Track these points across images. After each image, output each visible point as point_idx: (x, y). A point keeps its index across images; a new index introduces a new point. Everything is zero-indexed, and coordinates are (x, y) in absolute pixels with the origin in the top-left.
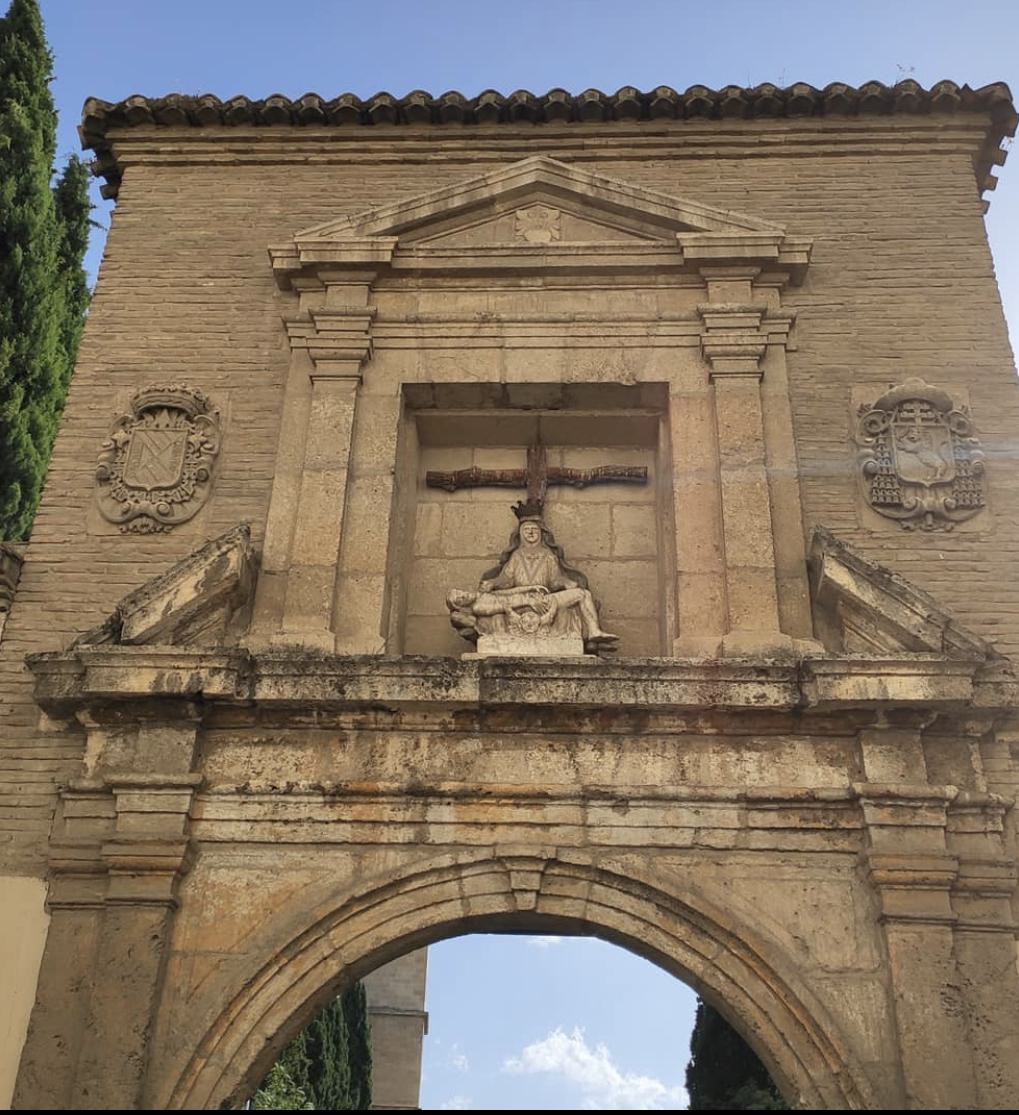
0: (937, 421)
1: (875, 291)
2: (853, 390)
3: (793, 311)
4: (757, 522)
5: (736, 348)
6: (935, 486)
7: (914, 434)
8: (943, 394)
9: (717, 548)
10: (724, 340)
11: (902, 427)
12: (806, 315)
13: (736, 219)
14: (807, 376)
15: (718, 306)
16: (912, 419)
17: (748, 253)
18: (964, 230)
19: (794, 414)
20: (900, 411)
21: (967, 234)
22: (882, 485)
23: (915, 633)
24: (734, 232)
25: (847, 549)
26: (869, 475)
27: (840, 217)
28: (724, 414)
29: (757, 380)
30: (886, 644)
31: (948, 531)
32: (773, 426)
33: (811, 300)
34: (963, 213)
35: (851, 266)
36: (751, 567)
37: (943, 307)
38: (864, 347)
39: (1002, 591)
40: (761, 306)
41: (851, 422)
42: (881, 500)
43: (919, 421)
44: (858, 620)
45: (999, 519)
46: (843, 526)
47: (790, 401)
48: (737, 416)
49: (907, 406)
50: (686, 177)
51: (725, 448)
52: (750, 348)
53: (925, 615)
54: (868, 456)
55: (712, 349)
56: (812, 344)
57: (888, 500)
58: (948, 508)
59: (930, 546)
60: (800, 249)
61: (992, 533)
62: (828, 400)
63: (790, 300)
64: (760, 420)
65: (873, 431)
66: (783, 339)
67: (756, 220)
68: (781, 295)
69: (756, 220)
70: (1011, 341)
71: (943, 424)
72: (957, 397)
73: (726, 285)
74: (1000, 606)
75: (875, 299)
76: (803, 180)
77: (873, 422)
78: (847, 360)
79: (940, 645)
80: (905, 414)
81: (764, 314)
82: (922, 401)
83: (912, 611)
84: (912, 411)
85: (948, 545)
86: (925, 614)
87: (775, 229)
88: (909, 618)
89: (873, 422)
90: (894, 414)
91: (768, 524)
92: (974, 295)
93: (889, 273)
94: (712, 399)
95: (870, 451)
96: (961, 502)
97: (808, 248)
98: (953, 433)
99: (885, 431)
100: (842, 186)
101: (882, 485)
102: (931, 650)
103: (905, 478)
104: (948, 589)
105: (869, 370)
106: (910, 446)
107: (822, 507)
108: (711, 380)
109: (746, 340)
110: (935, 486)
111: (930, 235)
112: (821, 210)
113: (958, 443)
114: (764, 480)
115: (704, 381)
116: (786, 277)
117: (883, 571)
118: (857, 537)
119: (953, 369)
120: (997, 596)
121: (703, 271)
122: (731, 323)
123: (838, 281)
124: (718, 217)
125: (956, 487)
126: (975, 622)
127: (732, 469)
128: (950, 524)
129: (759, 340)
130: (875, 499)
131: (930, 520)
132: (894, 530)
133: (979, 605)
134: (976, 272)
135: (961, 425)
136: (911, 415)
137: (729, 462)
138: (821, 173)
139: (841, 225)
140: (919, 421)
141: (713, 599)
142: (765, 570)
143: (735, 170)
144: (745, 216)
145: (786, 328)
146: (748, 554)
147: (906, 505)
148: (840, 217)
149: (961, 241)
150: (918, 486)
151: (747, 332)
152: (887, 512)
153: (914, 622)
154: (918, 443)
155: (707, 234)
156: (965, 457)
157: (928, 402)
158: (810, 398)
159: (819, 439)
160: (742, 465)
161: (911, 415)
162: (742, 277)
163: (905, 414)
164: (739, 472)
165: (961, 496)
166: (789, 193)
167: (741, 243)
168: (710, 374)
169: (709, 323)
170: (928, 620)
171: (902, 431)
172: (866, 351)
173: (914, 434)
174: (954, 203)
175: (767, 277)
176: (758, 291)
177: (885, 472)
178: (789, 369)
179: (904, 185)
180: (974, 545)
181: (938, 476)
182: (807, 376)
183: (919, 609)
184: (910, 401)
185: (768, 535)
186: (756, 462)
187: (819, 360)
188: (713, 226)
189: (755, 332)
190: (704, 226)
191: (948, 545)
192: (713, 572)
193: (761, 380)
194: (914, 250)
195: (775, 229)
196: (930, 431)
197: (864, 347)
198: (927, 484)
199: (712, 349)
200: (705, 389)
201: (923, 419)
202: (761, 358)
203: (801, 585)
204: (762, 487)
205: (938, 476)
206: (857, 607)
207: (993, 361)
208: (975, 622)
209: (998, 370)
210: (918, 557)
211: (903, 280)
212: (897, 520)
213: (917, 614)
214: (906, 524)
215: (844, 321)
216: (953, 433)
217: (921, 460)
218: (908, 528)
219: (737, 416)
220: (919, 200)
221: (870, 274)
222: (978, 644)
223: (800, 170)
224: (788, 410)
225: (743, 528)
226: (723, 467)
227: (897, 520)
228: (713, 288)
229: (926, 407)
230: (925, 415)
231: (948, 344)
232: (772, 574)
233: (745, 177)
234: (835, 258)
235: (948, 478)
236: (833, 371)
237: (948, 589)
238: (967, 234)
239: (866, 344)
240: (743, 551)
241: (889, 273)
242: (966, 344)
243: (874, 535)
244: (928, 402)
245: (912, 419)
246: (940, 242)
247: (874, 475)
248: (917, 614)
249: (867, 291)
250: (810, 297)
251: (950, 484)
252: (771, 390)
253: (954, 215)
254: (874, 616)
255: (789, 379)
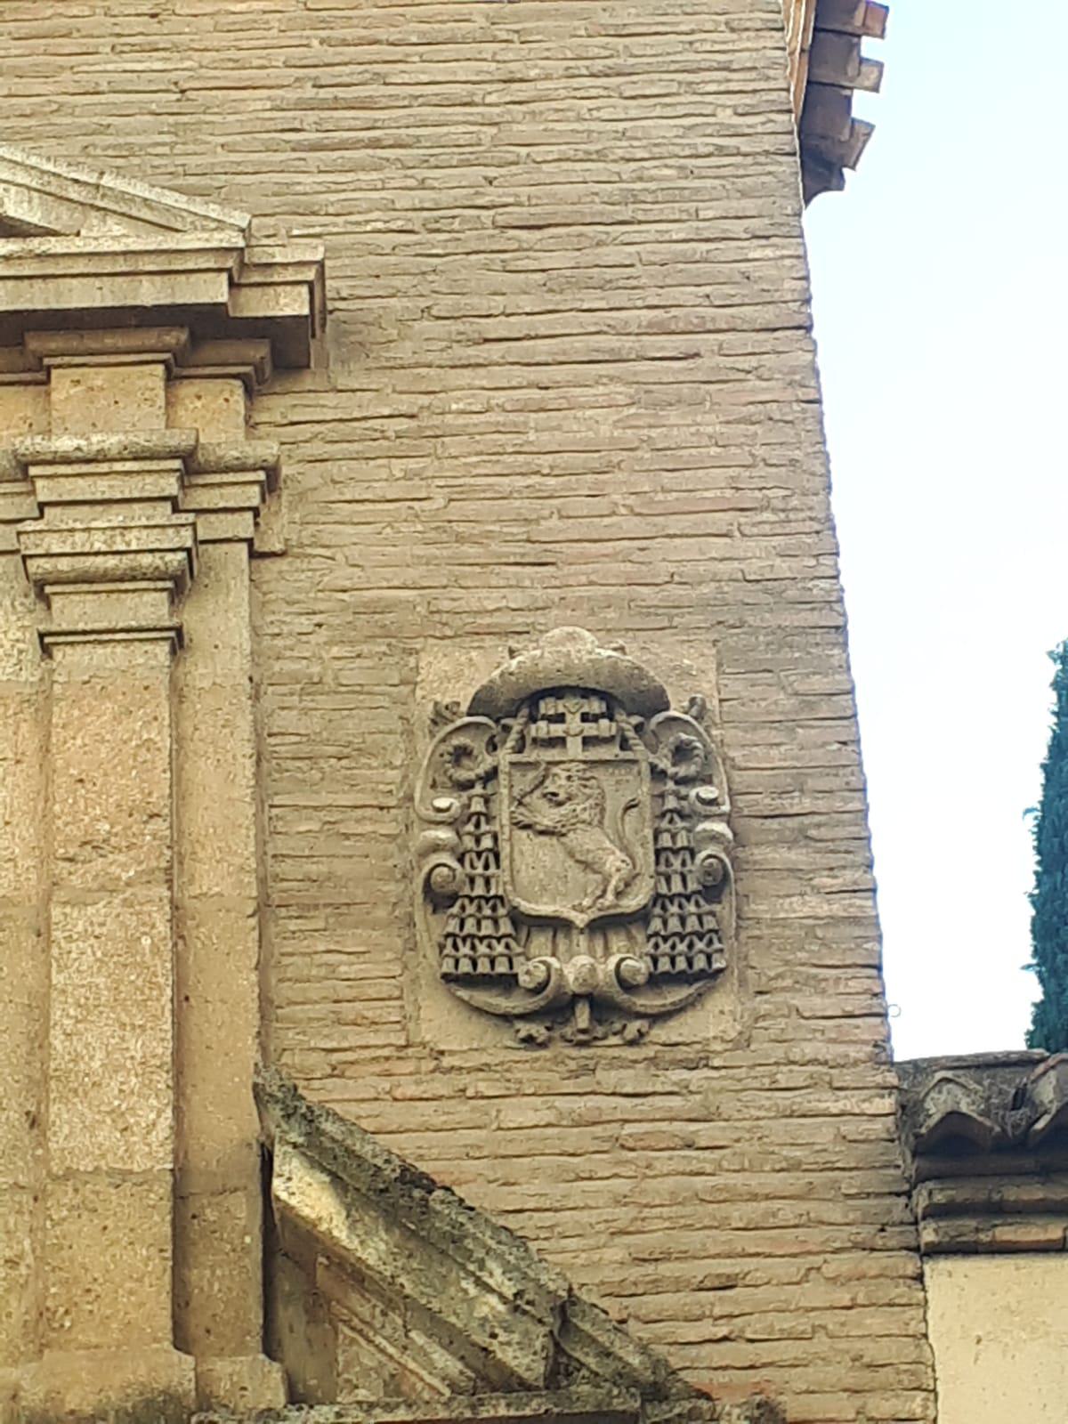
0: (624, 745)
1: (501, 375)
2: (425, 660)
3: (267, 449)
4: (135, 1047)
5: (111, 562)
6: (603, 926)
7: (558, 784)
8: (637, 672)
9: (34, 1121)
10: (80, 542)
11: (533, 765)
12: (317, 449)
13: (123, 196)
14: (305, 623)
15: (65, 444)
16: (559, 742)
17: (149, 294)
18: (744, 194)
19: (261, 734)
20: (533, 719)
21: (749, 206)
22: (470, 927)
23: (481, 1339)
24: (111, 235)
25: (328, 1126)
26: (439, 898)
27: (424, 162)
28: (72, 749)
29: (166, 647)
30: (431, 1366)
31: (632, 1043)
32: (202, 771)
33: (332, 404)
34: (744, 145)
35: (444, 305)
36: (111, 1173)
37: (673, 415)
38: (460, 539)
39: (754, 1197)
40: (179, 439)
41: (411, 752)
42: (465, 966)
43: (574, 748)
44: (364, 1307)
45: (763, 1005)
46: (373, 1039)
47: (256, 697)
48: (104, 751)
49: (547, 707)
50: (17, 48)
51: (68, 840)
52: (146, 560)
53: (509, 1293)
54: (436, 848)
55: (46, 564)
56: (328, 533)
57: (484, 967)
58: (626, 985)
59: (585, 1083)
60: (290, 275)
61: (743, 1042)
62: (360, 690)
63: (276, 407)
64: (162, 761)
65: (463, 775)
66: (242, 525)
67: (170, 198)
68: (249, 393)
69: (170, 198)
70: (835, 509)
71: (639, 750)
72: (686, 673)
73: (99, 377)
74: (748, 1241)
75: (500, 397)
76: (330, 54)
77: (461, 754)
78: (411, 575)
79: (540, 1368)
80: (542, 729)
81: (191, 465)
82: (586, 693)
83: (479, 1282)
84: (560, 718)
85: (630, 1080)
86: (509, 1290)
87: (221, 225)
88: (470, 1302)
89: (461, 754)
90: (516, 724)
91: (164, 1050)
92: (754, 383)
93: (542, 324)
94: (42, 701)
95: (444, 834)
96: (664, 965)
97: (310, 274)
98: (658, 774)
99: (493, 774)
100: (438, 71)
101: (470, 927)
102: (524, 1386)
103: (527, 907)
104: (620, 1201)
105: (471, 600)
106: (548, 816)
107: (314, 991)
108: (46, 651)
109: (134, 540)
110: (603, 926)
111: (656, 211)
112: (375, 144)
113: (671, 803)
114: (163, 928)
115: (34, 650)
116: (260, 351)
117: (412, 1179)
118: (409, 1066)
119: (680, 591)
120: (739, 1213)
121: (34, 344)
122: (102, 489)
123: (404, 352)
124: (73, 193)
125: (656, 924)
126: (678, 1285)
127: (79, 903)
128: (633, 1027)
129: (170, 539)
130: (448, 966)
131: (583, 1017)
132: (497, 1045)
133: (693, 1240)
134: (767, 315)
135: (682, 752)
136: (557, 730)
137: (75, 880)
138: (381, 34)
139: (422, 185)
140: (574, 748)
141: (12, 1263)
142: (146, 1179)
143: (154, 25)
144: (140, 189)
145: (253, 496)
146: (107, 1135)
147: (524, 979)
148: (424, 162)
149: (737, 227)
150: (557, 925)
151: (140, 514)
152: (482, 998)
153: (482, 1311)
154: (567, 807)
155: (36, 244)
156: (682, 841)
157: (602, 695)
158: (313, 685)
159: (324, 799)
160: (109, 888)
161: (557, 730)
162: (140, 356)
163: (542, 729)
164: (97, 911)
165: (665, 948)
166: (291, 95)
167: (129, 265)
168: (42, 636)
169: (44, 491)
170: (516, 1305)
171: (531, 775)
172: (468, 549)
173: (558, 783)
174: (725, 116)
175: (209, 352)
176: (187, 390)
177: (479, 890)
178: (259, 605)
179: (598, 65)
180: (696, 1077)
181: (610, 897)
182: (305, 623)
183: (497, 1278)
184: (558, 692)
185: (163, 1079)
186: (147, 878)
187: (343, 576)
188: (60, 217)
189: (163, 513)
190: (34, 217)
191: (630, 1080)
192: (17, 1186)
193: (178, 641)
194: (612, 254)
195: (221, 225)
196: (598, 773)
197: (460, 539)
198: (580, 919)
199: (46, 564)
200: (30, 675)
201: (587, 742)
202: (179, 586)
203: (243, 1212)
204: (155, 950)
205: (610, 897)
206: (357, 1276)
207: (783, 567)
208: (678, 1285)
209: (792, 593)
210: (550, 1116)
211: (578, 343)
212: (507, 1018)
213: (491, 1290)
214: (525, 1029)
215: (412, 464)
216: (658, 774)
217: (571, 854)
218: (529, 1040)
219: (104, 751)
220: (634, 108)
221: (494, 328)
222: (635, 1361)
223: (326, 24)
224: (244, 724)
225: (96, 1064)
226: (60, 895)
227: (507, 1018)
228: (62, 384)
229: (596, 706)
230: (590, 729)
231: (676, 524)
232: (163, 1189)
233: (175, 48)
234: (397, 282)
235: (632, 903)
236: (373, 609)
237: (620, 1201)
238: (749, 206)
239: (461, 528)
240: (90, 1129)
241: (542, 324)
242: (722, 520)
243: (447, 1061)
244: (602, 695)
245: (559, 742)
246: (678, 231)
247: (454, 898)
248: (491, 1290)
249: (481, 378)
250: (331, 399)
251: (642, 916)
252: (199, 672)
253: (721, 151)
254: (393, 1299)
255: (255, 632)
